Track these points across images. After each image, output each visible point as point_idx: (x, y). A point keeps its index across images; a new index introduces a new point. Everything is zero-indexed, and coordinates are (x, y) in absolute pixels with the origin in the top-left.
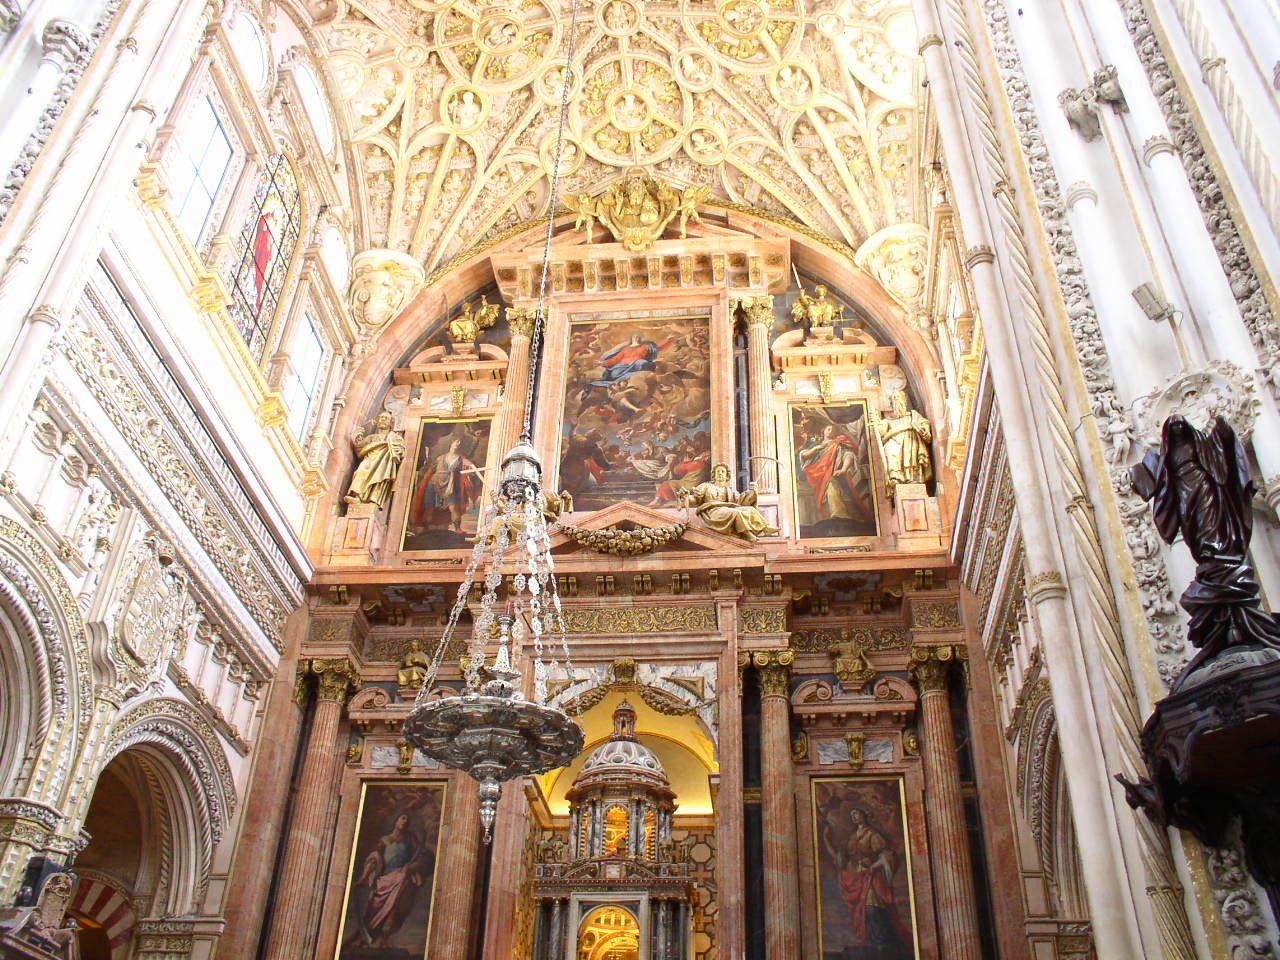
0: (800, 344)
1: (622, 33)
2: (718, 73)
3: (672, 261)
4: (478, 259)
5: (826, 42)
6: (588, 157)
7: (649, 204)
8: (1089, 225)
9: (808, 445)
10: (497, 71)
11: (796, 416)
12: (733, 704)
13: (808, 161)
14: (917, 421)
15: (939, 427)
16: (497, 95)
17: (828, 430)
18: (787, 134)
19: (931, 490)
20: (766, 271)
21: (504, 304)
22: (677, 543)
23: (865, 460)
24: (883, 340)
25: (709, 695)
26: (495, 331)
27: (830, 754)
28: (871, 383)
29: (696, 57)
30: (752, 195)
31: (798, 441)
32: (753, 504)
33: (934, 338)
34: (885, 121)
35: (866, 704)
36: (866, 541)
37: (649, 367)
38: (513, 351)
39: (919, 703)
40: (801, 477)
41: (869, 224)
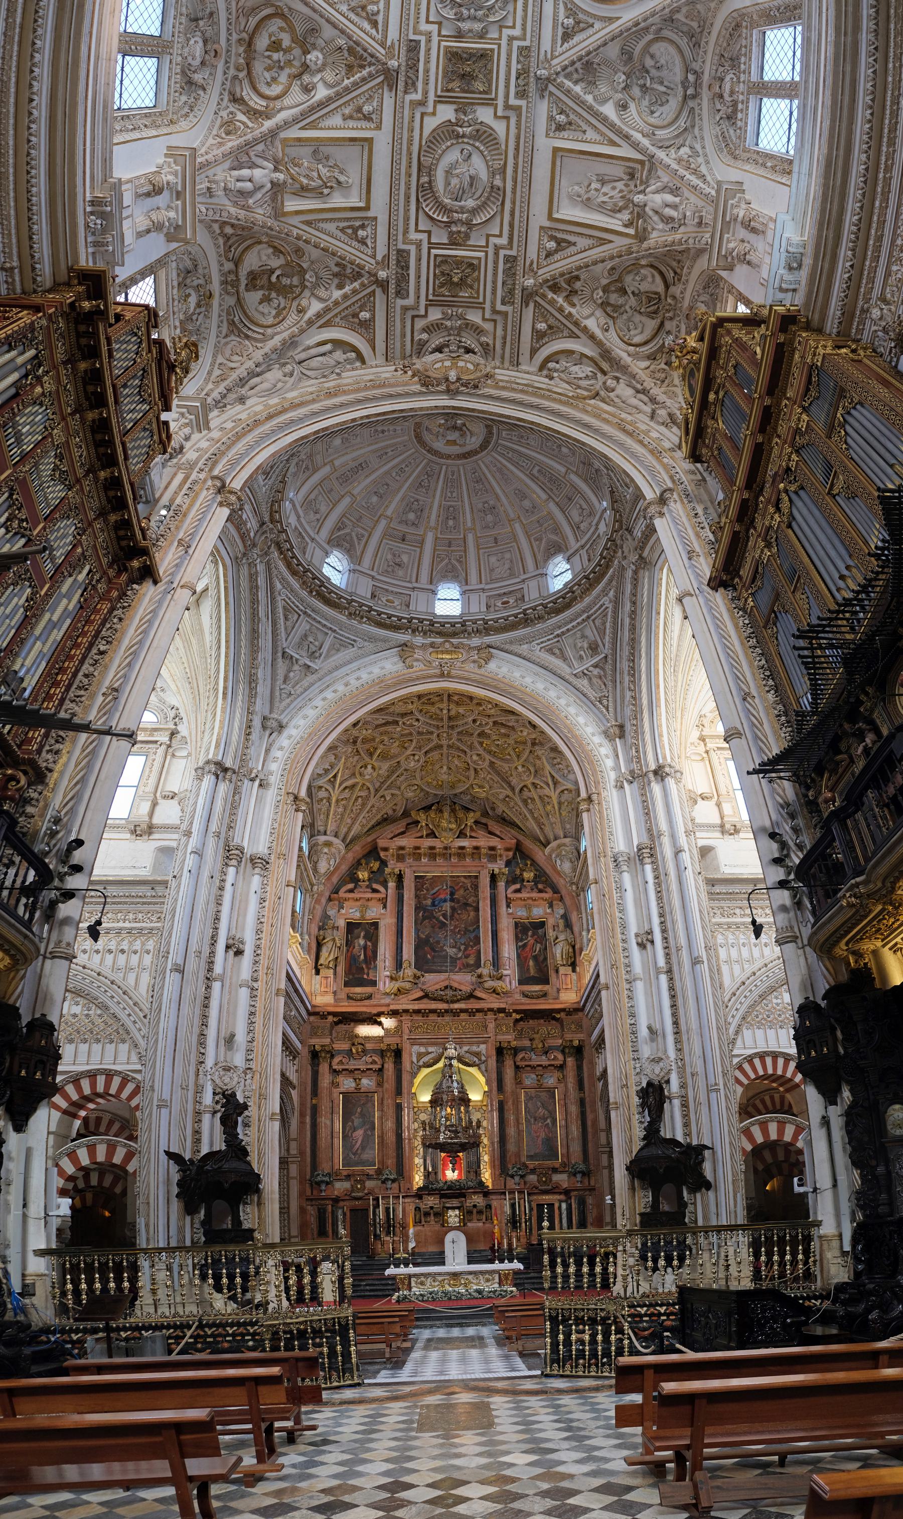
0: (518, 891)
1: (444, 742)
2: (487, 763)
3: (462, 848)
4: (370, 839)
5: (539, 759)
6: (422, 790)
7: (453, 820)
8: (639, 987)
9: (522, 940)
10: (384, 757)
11: (516, 924)
12: (492, 1062)
13: (525, 802)
14: (570, 938)
15: (578, 940)
16: (385, 766)
17: (530, 933)
18: (517, 790)
19: (574, 971)
20: (505, 854)
21: (384, 863)
22: (471, 996)
23: (546, 949)
24: (556, 891)
25: (483, 1058)
26: (379, 877)
27: (529, 1079)
28: (549, 911)
29: (478, 755)
30: (499, 811)
31: (517, 939)
32: (500, 978)
33: (578, 895)
34: (562, 791)
35: (544, 1061)
36: (546, 988)
37: (452, 900)
38: (390, 891)
39: (565, 1061)
40: (519, 956)
41: (552, 837)
